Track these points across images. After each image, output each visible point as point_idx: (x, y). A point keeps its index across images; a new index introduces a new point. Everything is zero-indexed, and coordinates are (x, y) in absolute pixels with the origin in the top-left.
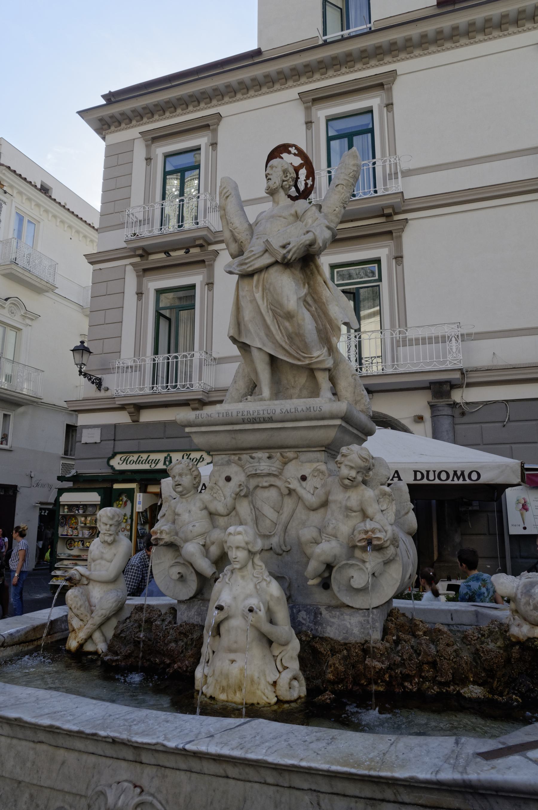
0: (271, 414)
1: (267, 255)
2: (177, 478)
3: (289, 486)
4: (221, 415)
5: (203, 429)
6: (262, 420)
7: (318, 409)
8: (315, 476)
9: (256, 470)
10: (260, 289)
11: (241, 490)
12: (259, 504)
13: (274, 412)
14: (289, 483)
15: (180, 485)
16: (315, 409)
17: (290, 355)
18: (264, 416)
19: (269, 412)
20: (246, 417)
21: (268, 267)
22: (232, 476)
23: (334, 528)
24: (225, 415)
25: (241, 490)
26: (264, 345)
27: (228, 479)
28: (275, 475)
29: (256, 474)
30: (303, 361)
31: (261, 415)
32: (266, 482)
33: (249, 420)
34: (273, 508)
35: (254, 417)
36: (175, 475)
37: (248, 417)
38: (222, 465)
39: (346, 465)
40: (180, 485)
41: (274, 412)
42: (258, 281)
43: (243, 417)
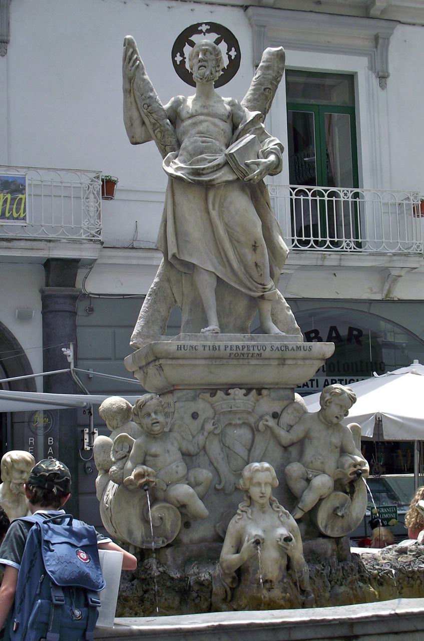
0: (262, 350)
1: (225, 170)
2: (153, 415)
3: (267, 423)
4: (207, 348)
5: (181, 362)
6: (250, 356)
7: (308, 348)
8: (289, 414)
9: (231, 408)
10: (217, 206)
11: (216, 428)
12: (228, 442)
13: (264, 349)
14: (267, 421)
15: (158, 422)
16: (305, 348)
17: (241, 283)
18: (254, 352)
19: (259, 349)
20: (234, 352)
21: (228, 183)
22: (200, 413)
23: (322, 463)
24: (211, 348)
25: (216, 428)
26: (216, 269)
27: (195, 416)
28: (249, 413)
29: (231, 411)
30: (254, 291)
31: (251, 352)
32: (239, 419)
33: (237, 355)
34: (244, 446)
35: (242, 352)
36: (150, 411)
37: (236, 352)
38: (187, 400)
39: (336, 404)
40: (158, 422)
41: (264, 349)
42: (215, 195)
43: (232, 352)
